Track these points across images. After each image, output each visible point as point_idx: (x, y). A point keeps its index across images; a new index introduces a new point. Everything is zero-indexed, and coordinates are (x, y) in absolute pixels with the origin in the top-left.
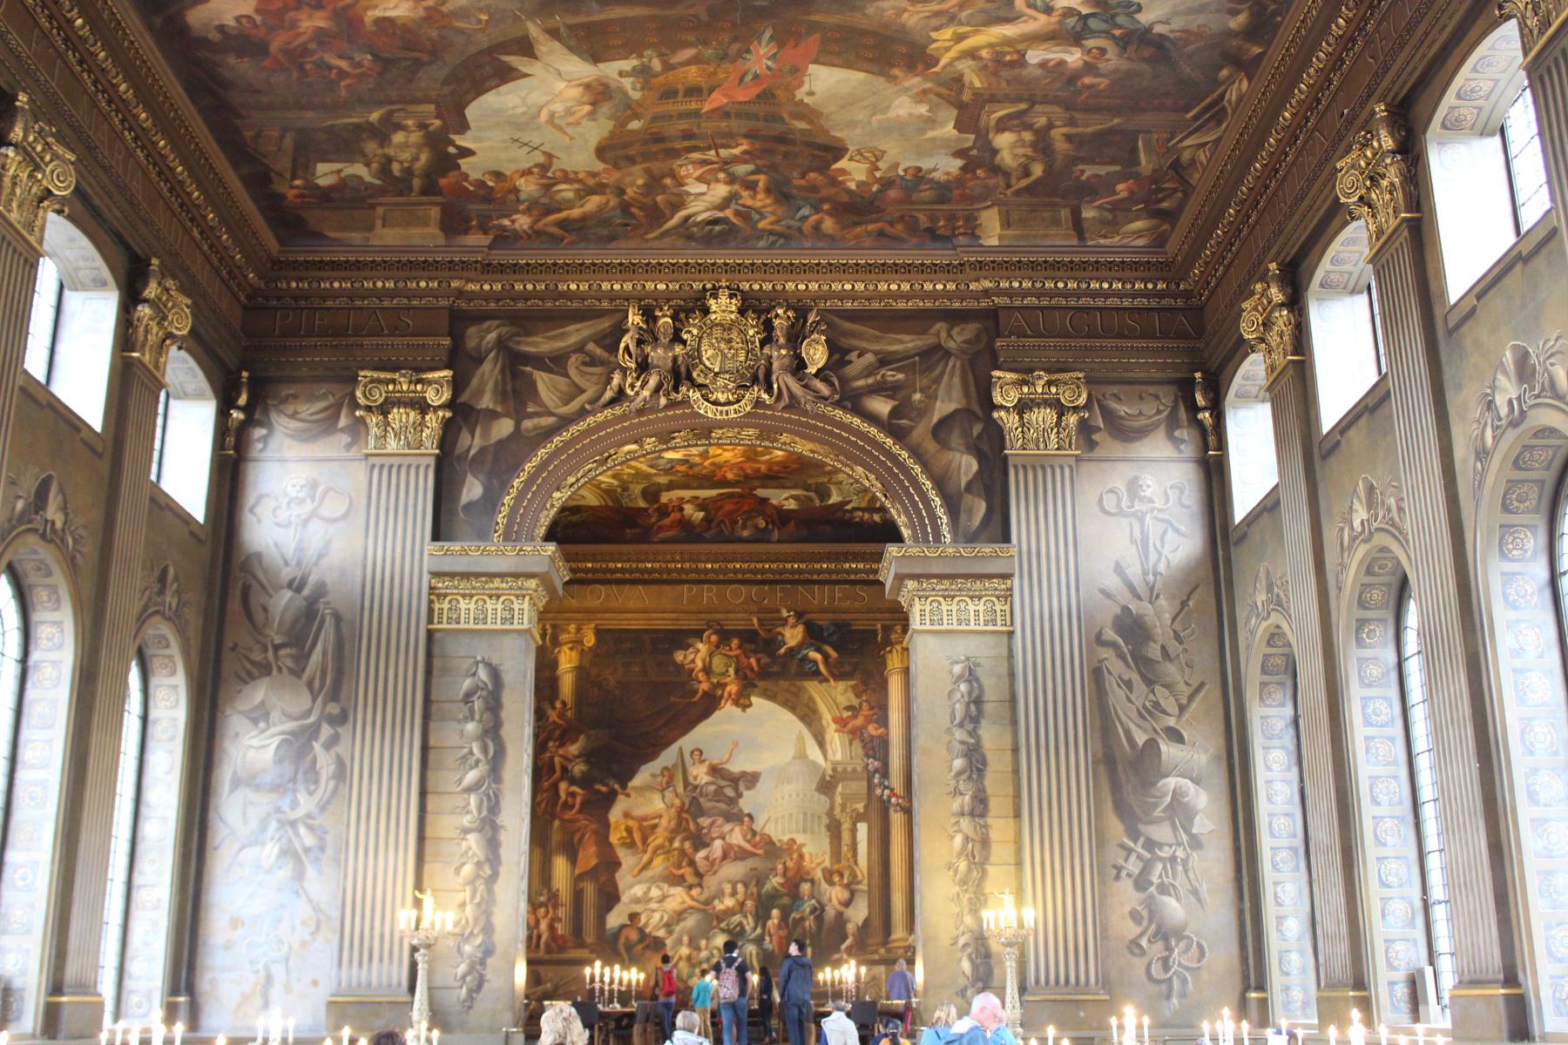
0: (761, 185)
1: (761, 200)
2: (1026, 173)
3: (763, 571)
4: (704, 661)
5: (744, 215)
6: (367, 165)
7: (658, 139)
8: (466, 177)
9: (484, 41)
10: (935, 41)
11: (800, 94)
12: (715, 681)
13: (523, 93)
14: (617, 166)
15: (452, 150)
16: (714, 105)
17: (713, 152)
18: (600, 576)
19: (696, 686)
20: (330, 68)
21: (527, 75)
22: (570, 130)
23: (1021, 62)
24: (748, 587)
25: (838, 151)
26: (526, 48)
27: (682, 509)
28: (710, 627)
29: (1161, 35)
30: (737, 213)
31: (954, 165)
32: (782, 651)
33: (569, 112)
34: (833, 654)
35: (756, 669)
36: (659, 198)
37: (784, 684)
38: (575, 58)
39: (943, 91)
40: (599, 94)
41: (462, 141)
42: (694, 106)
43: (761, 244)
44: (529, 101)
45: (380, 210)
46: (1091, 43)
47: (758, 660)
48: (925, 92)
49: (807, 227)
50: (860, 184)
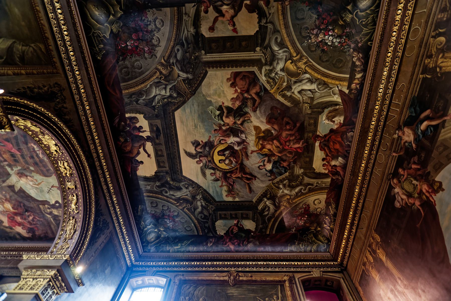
3: (374, 140)
4: (403, 194)
7: (36, 164)
9: (11, 194)
12: (416, 195)
17: (38, 152)
18: (359, 212)
19: (415, 208)
21: (21, 187)
22: (40, 182)
24: (380, 150)
26: (12, 187)
27: (335, 166)
28: (389, 180)
32: (414, 145)
33: (32, 181)
34: (427, 112)
35: (419, 167)
37: (435, 153)
38: (10, 178)
40: (21, 174)
44: (31, 188)
47: (414, 163)
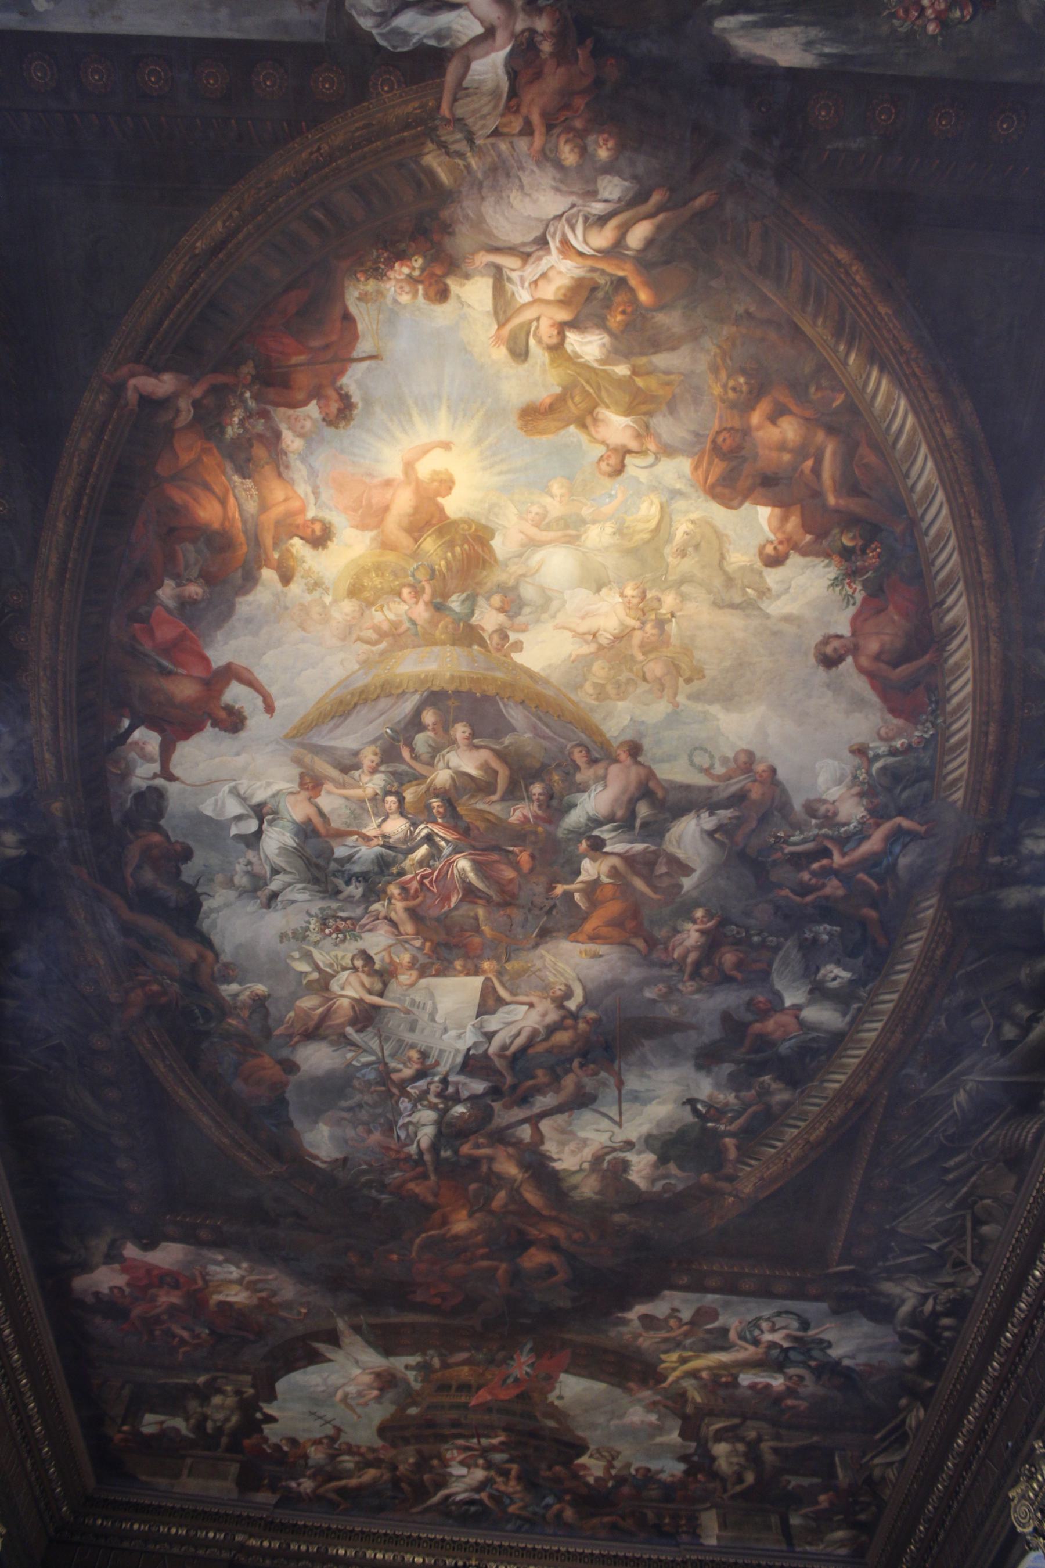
0: (513, 1473)
1: (512, 1487)
2: (740, 1479)
5: (497, 1498)
6: (187, 1420)
7: (430, 1424)
8: (266, 1440)
10: (664, 1362)
11: (552, 1397)
13: (326, 1374)
14: (394, 1445)
15: (259, 1415)
16: (480, 1400)
17: (475, 1440)
20: (174, 1336)
21: (330, 1360)
22: (359, 1410)
23: (734, 1384)
25: (580, 1448)
26: (333, 1339)
29: (848, 1368)
30: (491, 1496)
31: (678, 1468)
33: (360, 1394)
36: (426, 1477)
38: (371, 1350)
39: (670, 1403)
40: (386, 1381)
41: (270, 1409)
42: (463, 1399)
43: (509, 1527)
44: (330, 1382)
45: (189, 1461)
46: (792, 1371)
48: (655, 1403)
49: (550, 1514)
50: (597, 1479)
